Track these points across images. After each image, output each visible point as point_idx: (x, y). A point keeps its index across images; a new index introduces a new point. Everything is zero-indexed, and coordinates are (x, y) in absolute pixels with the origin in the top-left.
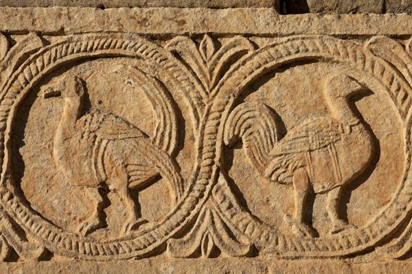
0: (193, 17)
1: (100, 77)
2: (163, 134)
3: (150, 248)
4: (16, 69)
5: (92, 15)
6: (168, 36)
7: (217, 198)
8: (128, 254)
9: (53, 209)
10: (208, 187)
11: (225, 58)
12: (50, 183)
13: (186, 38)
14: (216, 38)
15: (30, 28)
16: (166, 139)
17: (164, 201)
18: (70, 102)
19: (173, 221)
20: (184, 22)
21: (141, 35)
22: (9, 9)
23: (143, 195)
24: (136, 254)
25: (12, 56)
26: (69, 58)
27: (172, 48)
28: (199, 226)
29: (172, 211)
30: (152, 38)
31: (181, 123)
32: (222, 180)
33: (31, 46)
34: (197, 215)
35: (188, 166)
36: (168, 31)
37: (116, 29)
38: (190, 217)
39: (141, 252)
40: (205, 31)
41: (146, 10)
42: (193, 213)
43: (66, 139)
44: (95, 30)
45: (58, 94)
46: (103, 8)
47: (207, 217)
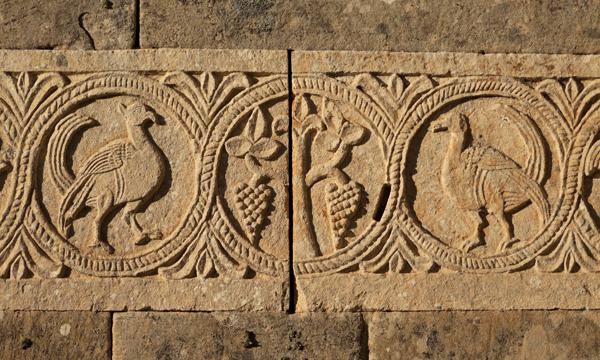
0: (560, 63)
1: (482, 114)
2: (533, 166)
3: (522, 264)
4: (410, 107)
5: (474, 60)
6: (539, 79)
7: (578, 221)
8: (503, 268)
9: (441, 229)
10: (571, 212)
11: (587, 99)
12: (438, 205)
13: (554, 81)
14: (579, 81)
15: (422, 71)
16: (536, 170)
17: (534, 224)
18: (455, 137)
19: (541, 241)
20: (552, 67)
21: (516, 78)
22: (404, 54)
23: (516, 218)
24: (510, 268)
25: (406, 96)
26: (455, 98)
27: (541, 90)
28: (562, 246)
29: (540, 233)
30: (525, 81)
31: (549, 155)
32: (582, 206)
33: (423, 87)
34: (561, 236)
35: (555, 194)
36: (539, 75)
37: (495, 73)
38: (555, 238)
39: (514, 267)
40: (571, 75)
41: (520, 56)
42: (558, 234)
43: (452, 169)
44: (477, 73)
45: (445, 129)
46: (483, 53)
47: (570, 238)
